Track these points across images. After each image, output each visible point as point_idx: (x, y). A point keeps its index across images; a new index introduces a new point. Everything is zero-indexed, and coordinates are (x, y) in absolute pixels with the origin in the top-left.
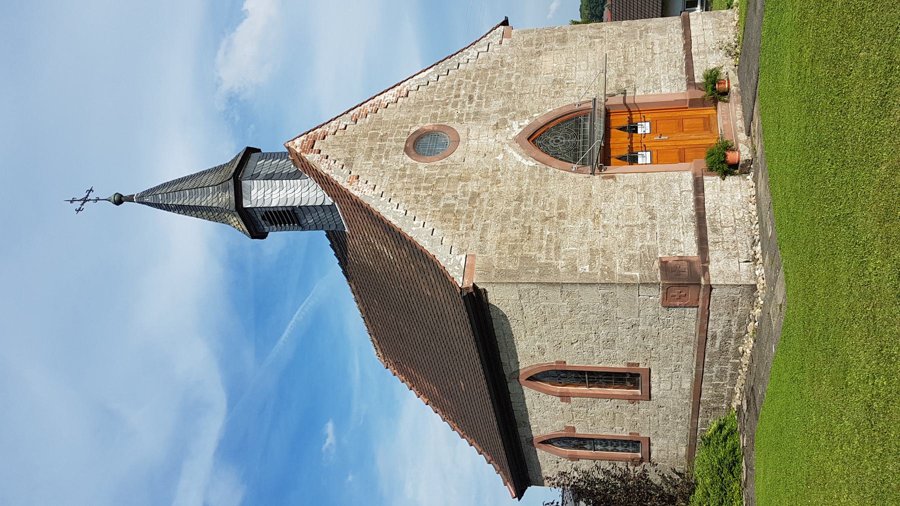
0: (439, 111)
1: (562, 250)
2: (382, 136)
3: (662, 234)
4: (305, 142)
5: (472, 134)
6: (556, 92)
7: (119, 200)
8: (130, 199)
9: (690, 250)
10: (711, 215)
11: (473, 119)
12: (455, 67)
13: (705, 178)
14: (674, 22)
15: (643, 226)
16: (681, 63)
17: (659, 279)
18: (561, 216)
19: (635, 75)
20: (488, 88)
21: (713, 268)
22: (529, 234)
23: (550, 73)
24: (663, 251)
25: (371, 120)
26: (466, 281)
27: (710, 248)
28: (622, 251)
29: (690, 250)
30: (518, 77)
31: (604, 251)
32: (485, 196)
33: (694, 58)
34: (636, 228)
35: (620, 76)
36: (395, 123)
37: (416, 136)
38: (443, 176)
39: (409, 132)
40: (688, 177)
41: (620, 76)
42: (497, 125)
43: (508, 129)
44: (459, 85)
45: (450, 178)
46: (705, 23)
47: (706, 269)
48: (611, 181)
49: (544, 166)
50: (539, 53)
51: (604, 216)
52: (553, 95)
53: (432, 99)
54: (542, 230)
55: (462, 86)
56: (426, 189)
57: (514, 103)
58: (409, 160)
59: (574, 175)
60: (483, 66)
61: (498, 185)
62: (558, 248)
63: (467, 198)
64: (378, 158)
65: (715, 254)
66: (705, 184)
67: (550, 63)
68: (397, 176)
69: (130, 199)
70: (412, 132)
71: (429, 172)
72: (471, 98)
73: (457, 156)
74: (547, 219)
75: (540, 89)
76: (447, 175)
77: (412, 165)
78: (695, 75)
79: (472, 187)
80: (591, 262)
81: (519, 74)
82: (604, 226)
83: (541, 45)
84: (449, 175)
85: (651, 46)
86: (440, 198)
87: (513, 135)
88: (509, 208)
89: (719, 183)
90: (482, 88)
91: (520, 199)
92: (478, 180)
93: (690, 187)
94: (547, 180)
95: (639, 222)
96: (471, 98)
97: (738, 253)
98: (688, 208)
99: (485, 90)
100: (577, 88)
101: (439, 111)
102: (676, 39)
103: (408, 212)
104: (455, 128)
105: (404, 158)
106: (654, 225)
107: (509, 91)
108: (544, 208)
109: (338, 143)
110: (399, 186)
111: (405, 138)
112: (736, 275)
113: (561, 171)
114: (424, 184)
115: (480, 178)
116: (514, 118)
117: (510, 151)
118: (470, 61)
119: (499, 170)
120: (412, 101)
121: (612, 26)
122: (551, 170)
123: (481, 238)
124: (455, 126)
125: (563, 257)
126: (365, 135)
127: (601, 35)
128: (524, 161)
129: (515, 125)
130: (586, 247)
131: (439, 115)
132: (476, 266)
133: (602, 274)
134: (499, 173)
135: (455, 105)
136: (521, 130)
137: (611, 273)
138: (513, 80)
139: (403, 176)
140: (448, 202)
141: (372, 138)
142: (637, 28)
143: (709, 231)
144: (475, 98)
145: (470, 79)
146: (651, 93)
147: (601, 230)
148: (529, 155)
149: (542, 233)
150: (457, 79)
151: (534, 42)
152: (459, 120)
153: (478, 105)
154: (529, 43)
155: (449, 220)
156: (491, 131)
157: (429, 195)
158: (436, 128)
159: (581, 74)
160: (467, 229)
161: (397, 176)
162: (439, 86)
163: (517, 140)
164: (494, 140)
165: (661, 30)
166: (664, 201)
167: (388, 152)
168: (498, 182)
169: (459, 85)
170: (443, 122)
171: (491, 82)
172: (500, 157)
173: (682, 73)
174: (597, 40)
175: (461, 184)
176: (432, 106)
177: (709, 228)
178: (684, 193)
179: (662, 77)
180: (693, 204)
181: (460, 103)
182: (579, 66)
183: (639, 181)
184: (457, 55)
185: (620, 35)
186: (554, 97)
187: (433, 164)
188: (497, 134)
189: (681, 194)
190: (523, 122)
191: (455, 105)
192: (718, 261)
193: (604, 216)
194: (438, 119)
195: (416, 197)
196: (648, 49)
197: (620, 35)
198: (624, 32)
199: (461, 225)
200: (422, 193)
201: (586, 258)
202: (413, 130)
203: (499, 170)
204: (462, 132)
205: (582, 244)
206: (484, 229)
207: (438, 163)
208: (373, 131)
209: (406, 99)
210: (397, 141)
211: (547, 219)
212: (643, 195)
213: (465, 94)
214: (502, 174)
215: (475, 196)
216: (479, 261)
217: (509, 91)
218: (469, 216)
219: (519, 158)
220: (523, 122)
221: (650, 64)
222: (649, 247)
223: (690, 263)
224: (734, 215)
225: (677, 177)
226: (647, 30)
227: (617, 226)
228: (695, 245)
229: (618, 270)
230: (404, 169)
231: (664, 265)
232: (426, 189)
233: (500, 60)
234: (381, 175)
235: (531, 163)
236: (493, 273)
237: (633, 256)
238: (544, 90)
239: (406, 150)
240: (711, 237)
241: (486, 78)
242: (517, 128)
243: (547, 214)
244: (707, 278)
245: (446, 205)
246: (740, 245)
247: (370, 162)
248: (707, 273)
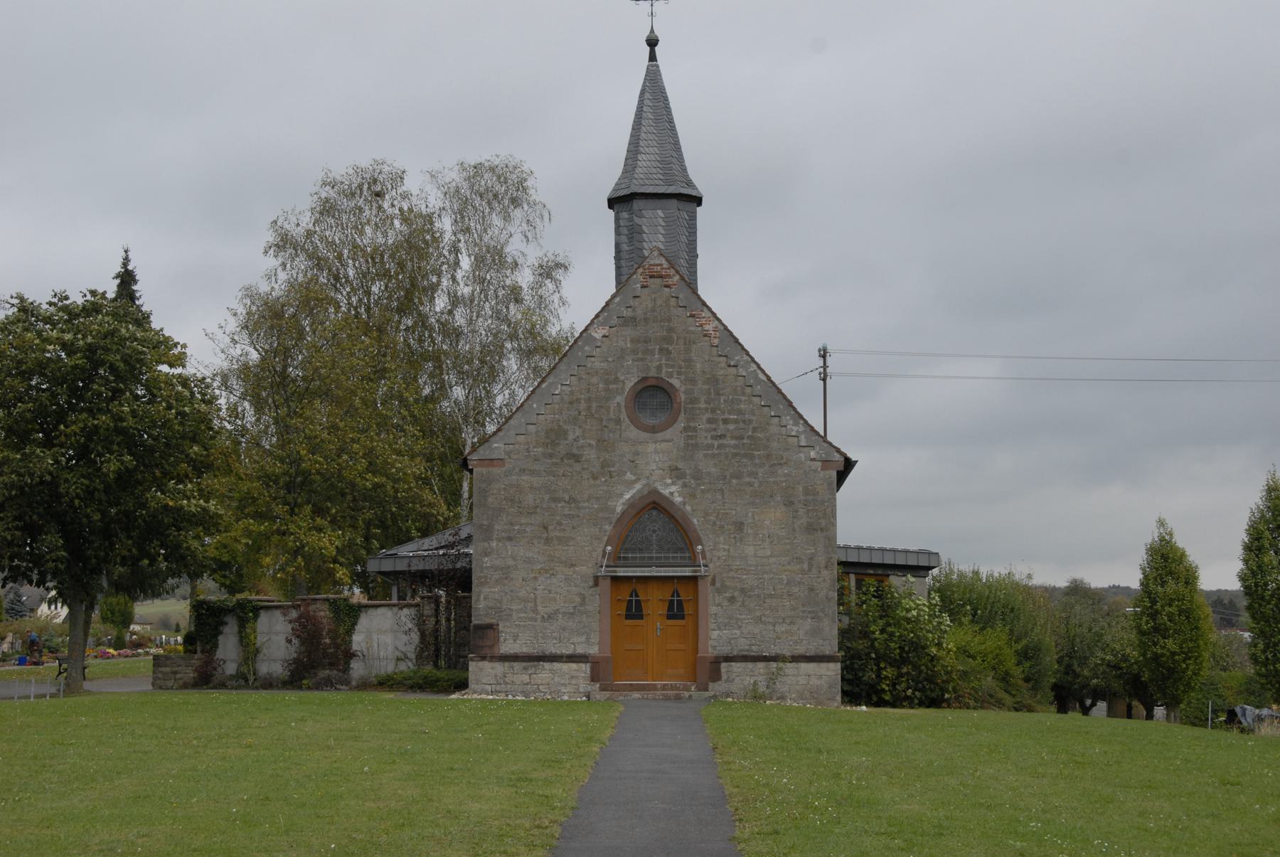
0: (703, 406)
1: (508, 543)
2: (667, 350)
3: (524, 626)
4: (659, 268)
5: (664, 445)
6: (722, 527)
7: (652, 43)
8: (653, 57)
9: (508, 646)
10: (543, 666)
11: (688, 444)
12: (773, 414)
13: (588, 665)
14: (830, 645)
15: (535, 611)
16: (755, 650)
17: (476, 622)
18: (548, 541)
19: (743, 605)
20: (735, 455)
21: (486, 665)
22: (528, 513)
23: (754, 518)
24: (505, 626)
25: (693, 332)
26: (475, 462)
27: (507, 664)
28: (506, 593)
29: (508, 646)
30: (750, 484)
31: (506, 578)
32: (578, 467)
33: (761, 665)
34: (532, 605)
35: (743, 591)
36: (689, 361)
37: (665, 387)
38: (604, 423)
39: (671, 377)
40: (594, 650)
41: (743, 591)
42: (677, 469)
43: (669, 481)
44: (744, 422)
45: (602, 430)
46: (820, 677)
47: (483, 658)
48: (591, 583)
49: (614, 520)
50: (789, 504)
51: (547, 578)
52: (718, 523)
53: (723, 394)
54: (531, 524)
55: (741, 425)
56: (589, 408)
57: (710, 483)
58: (629, 385)
59: (600, 550)
60: (775, 444)
61: (591, 480)
62: (510, 539)
63: (575, 451)
64: (634, 352)
65: (499, 668)
66: (581, 664)
67: (772, 517)
68: (607, 377)
69: (653, 57)
70: (671, 381)
71: (612, 408)
72: (722, 436)
73: (633, 433)
74: (546, 528)
75: (731, 509)
76: (606, 426)
77: (623, 389)
78: (733, 664)
79: (590, 454)
80: (496, 568)
81: (756, 485)
82: (535, 578)
83: (805, 505)
84: (606, 429)
85: (788, 621)
86: (575, 424)
87: (659, 487)
88: (561, 492)
89: (583, 675)
90: (736, 446)
91: (572, 500)
92: (598, 458)
93: (580, 650)
94: (595, 525)
95: (539, 608)
96: (722, 436)
97: (500, 684)
98: (553, 649)
99: (732, 450)
100: (726, 547)
101: (703, 406)
102: (798, 647)
103: (558, 397)
104: (675, 426)
105: (633, 379)
106: (536, 620)
107: (728, 477)
108: (559, 524)
109: (659, 302)
110: (594, 380)
111: (663, 375)
112: (478, 681)
113: (606, 538)
114: (594, 405)
115: (601, 460)
116: (685, 485)
117: (638, 486)
118: (783, 428)
119: (611, 477)
120: (721, 372)
121: (829, 581)
122: (608, 528)
123: (524, 470)
124: (681, 424)
125: (500, 544)
126: (671, 330)
127: (814, 571)
128: (622, 501)
129: (673, 489)
130: (510, 562)
131: (696, 406)
132: (491, 469)
133: (481, 577)
134: (608, 477)
135: (709, 421)
136: (668, 495)
137: (482, 584)
138: (747, 479)
139: (607, 382)
140: (570, 433)
141: (668, 340)
142: (821, 607)
143: (524, 664)
144: (721, 442)
145: (753, 432)
146: (713, 621)
147: (532, 576)
148: (631, 504)
149: (527, 524)
150: (754, 418)
151: (810, 498)
152: (686, 429)
153: (710, 447)
154: (807, 492)
155: (547, 437)
156: (670, 463)
157: (580, 413)
158: (675, 405)
159: (750, 550)
160: (535, 455)
161: (607, 377)
162: (743, 398)
163: (655, 492)
164: (654, 468)
165: (815, 632)
166: (564, 629)
167: (642, 360)
168: (595, 478)
169: (744, 422)
170: (685, 411)
171: (745, 455)
172: (629, 476)
173: (741, 650)
174: (806, 566)
175: (593, 443)
176: (713, 396)
177: (529, 664)
178: (573, 646)
179: (736, 631)
180: (559, 652)
181: (713, 426)
182: (764, 548)
183: (589, 608)
184: (793, 412)
185: (811, 590)
186: (714, 523)
187: (623, 410)
188: (664, 470)
189: (573, 643)
190: (679, 496)
191: (709, 421)
192: (492, 668)
193: (547, 578)
194: (690, 406)
195: (578, 400)
196: (784, 619)
197: (811, 590)
198: (817, 594)
199: (540, 449)
200: (583, 405)
201: (498, 562)
202: (675, 382)
203: (611, 477)
204: (668, 434)
205: (514, 558)
206: (532, 472)
207: (624, 416)
208: (675, 338)
209: (723, 365)
210: (659, 368)
211: (546, 528)
212: (572, 611)
213: (728, 430)
214: (606, 481)
215: (577, 458)
216: (496, 471)
217: (728, 477)
218: (551, 456)
219: (627, 496)
220: (679, 496)
221: (759, 620)
222: (510, 615)
223: (491, 647)
224: (542, 684)
225: (593, 641)
226: (816, 617)
227: (536, 589)
228: (512, 652)
229: (486, 590)
230: (616, 380)
231: (490, 627)
232: (589, 408)
233: (782, 462)
234: (610, 359)
235: (619, 509)
236: (484, 486)
237: (500, 602)
238: (727, 513)
239: (644, 379)
240: (517, 666)
241: (753, 450)
242: (672, 491)
243: (550, 528)
244: (475, 659)
245: (566, 432)
246: (509, 686)
247: (629, 345)
248: (478, 659)
